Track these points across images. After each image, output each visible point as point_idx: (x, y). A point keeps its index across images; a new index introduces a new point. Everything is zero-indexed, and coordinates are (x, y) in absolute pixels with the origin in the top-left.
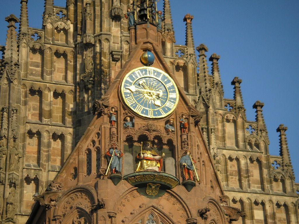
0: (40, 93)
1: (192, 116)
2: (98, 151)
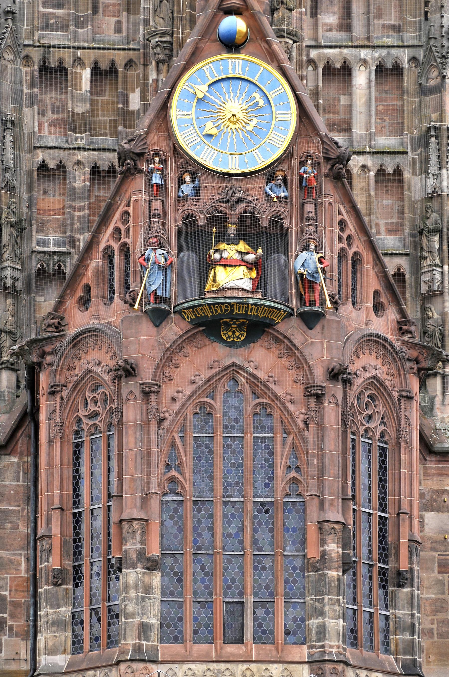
1: (327, 159)
2: (125, 250)
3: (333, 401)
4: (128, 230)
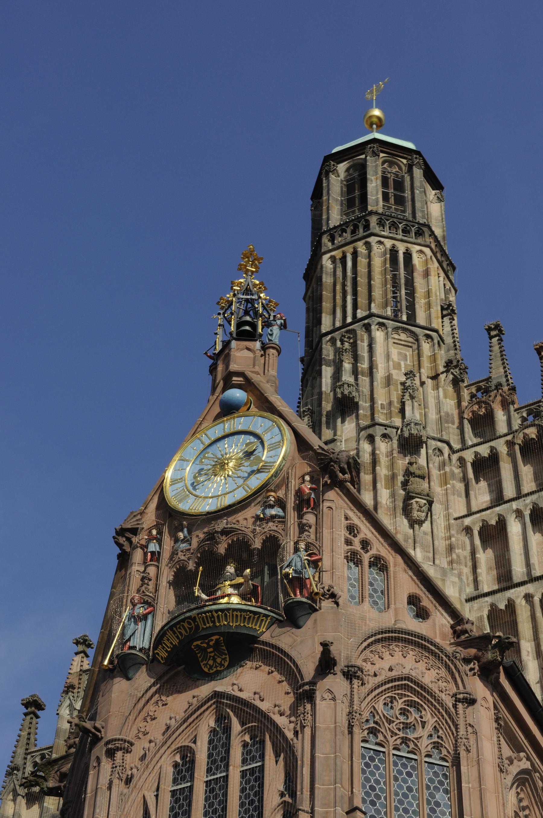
3: (327, 696)
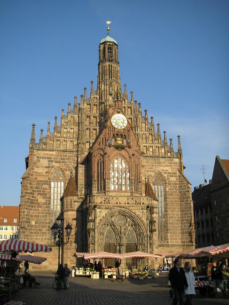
0: (90, 117)
4: (106, 135)
